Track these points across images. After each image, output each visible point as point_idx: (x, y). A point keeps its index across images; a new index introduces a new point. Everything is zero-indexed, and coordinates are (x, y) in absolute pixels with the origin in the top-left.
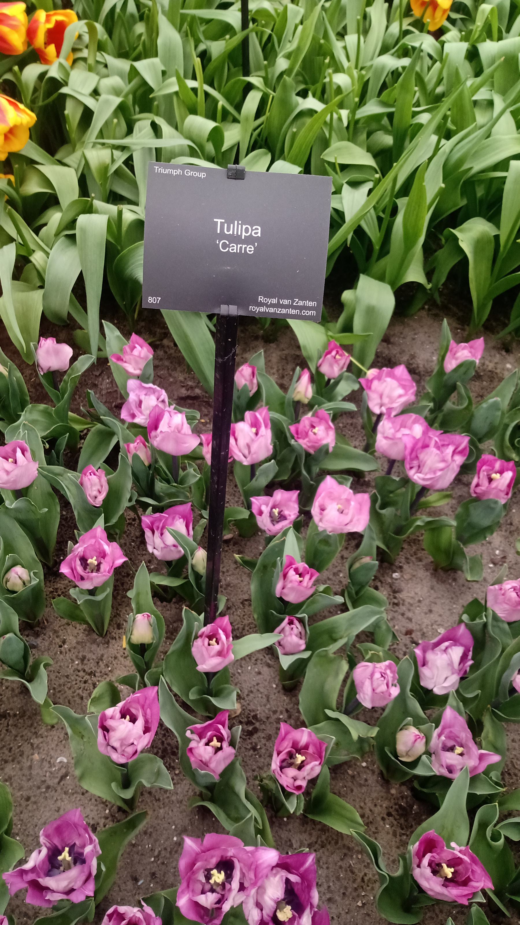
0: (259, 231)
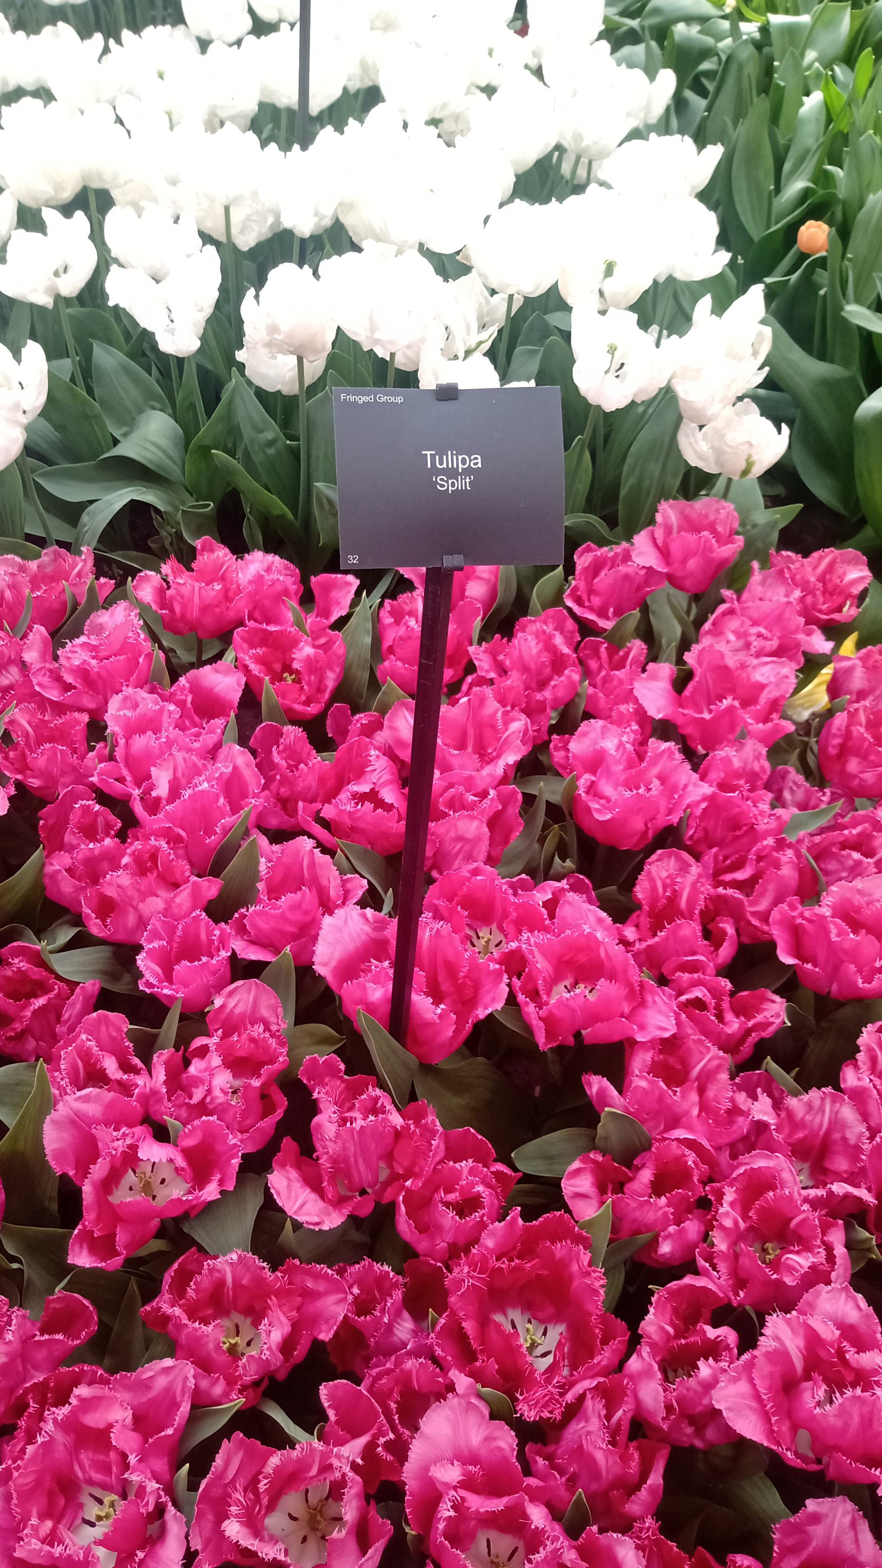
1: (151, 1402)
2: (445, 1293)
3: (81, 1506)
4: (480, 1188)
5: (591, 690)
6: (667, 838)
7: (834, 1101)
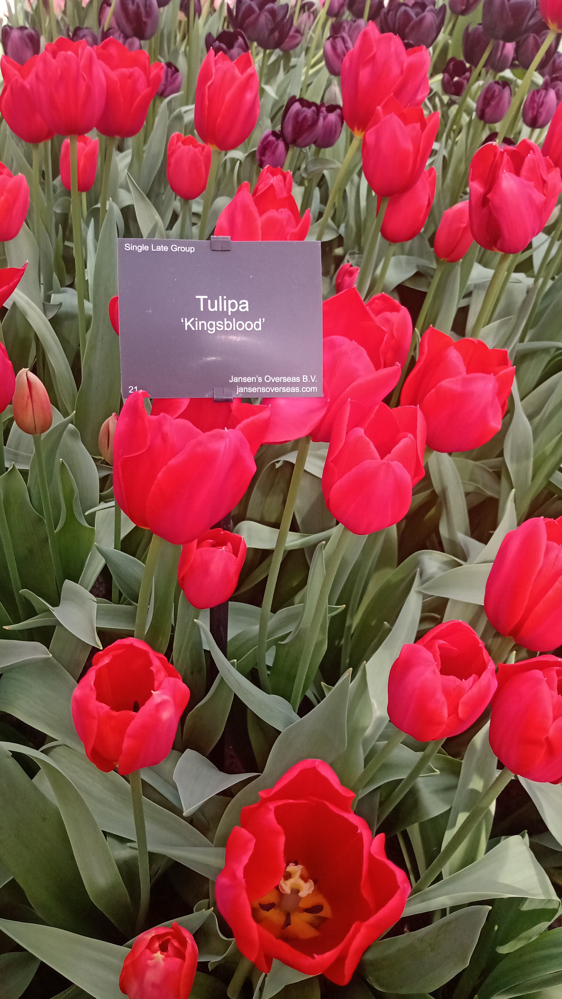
0: (247, 305)
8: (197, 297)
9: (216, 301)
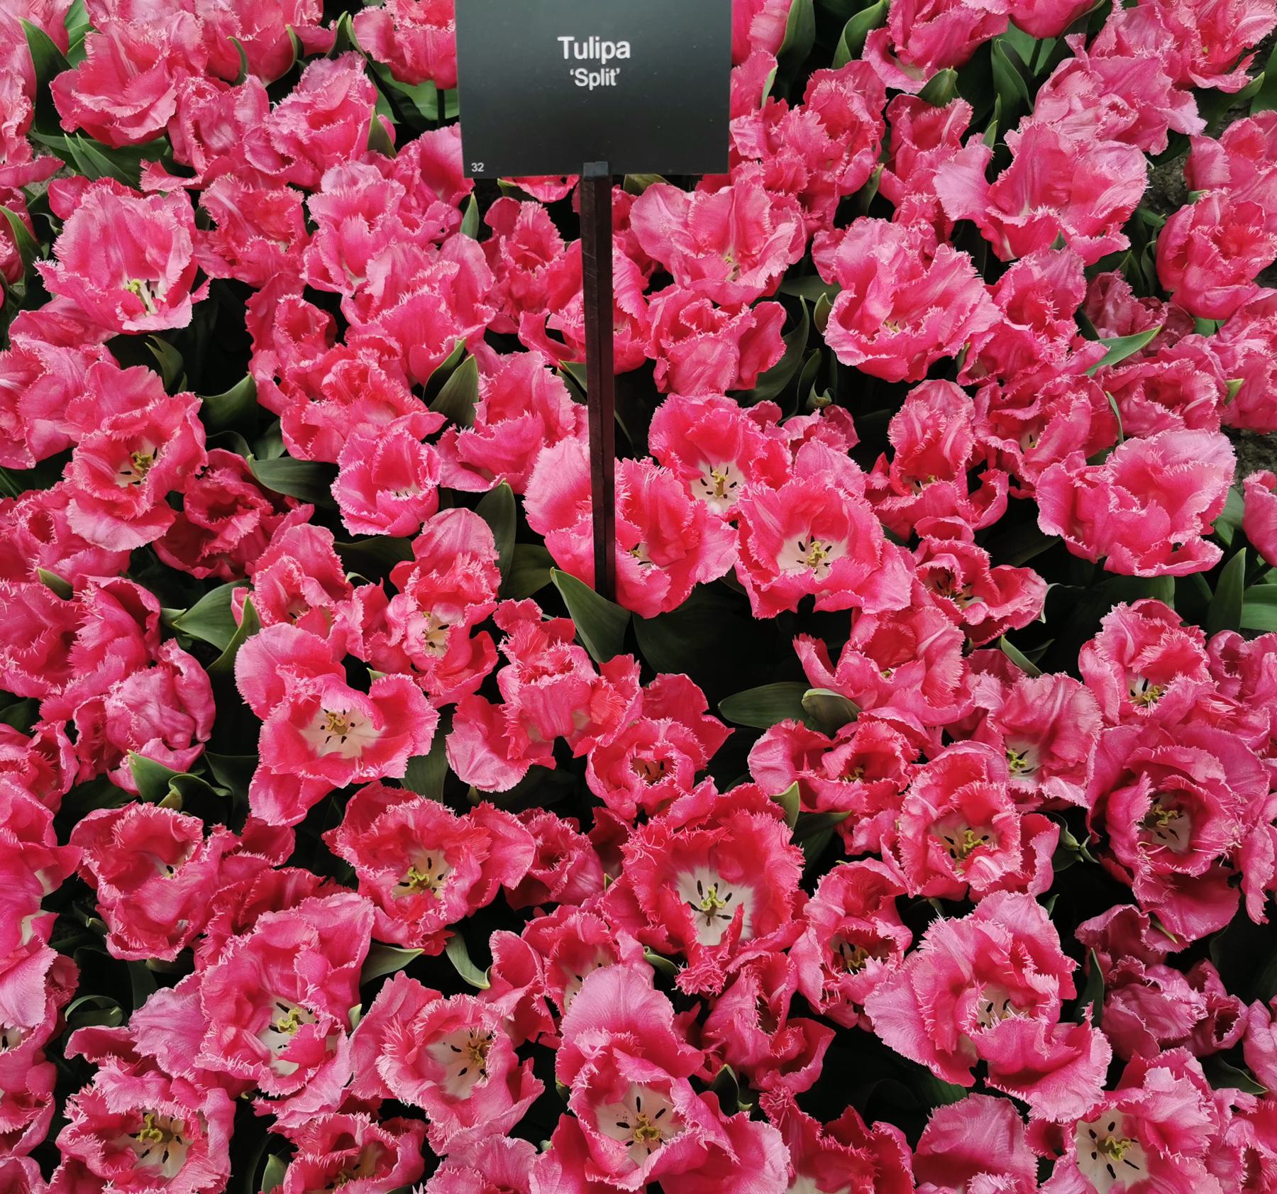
1: (337, 929)
2: (621, 856)
3: (271, 1011)
4: (674, 754)
5: (887, 173)
6: (944, 369)
7: (1068, 687)
8: (560, 39)
9: (585, 45)
